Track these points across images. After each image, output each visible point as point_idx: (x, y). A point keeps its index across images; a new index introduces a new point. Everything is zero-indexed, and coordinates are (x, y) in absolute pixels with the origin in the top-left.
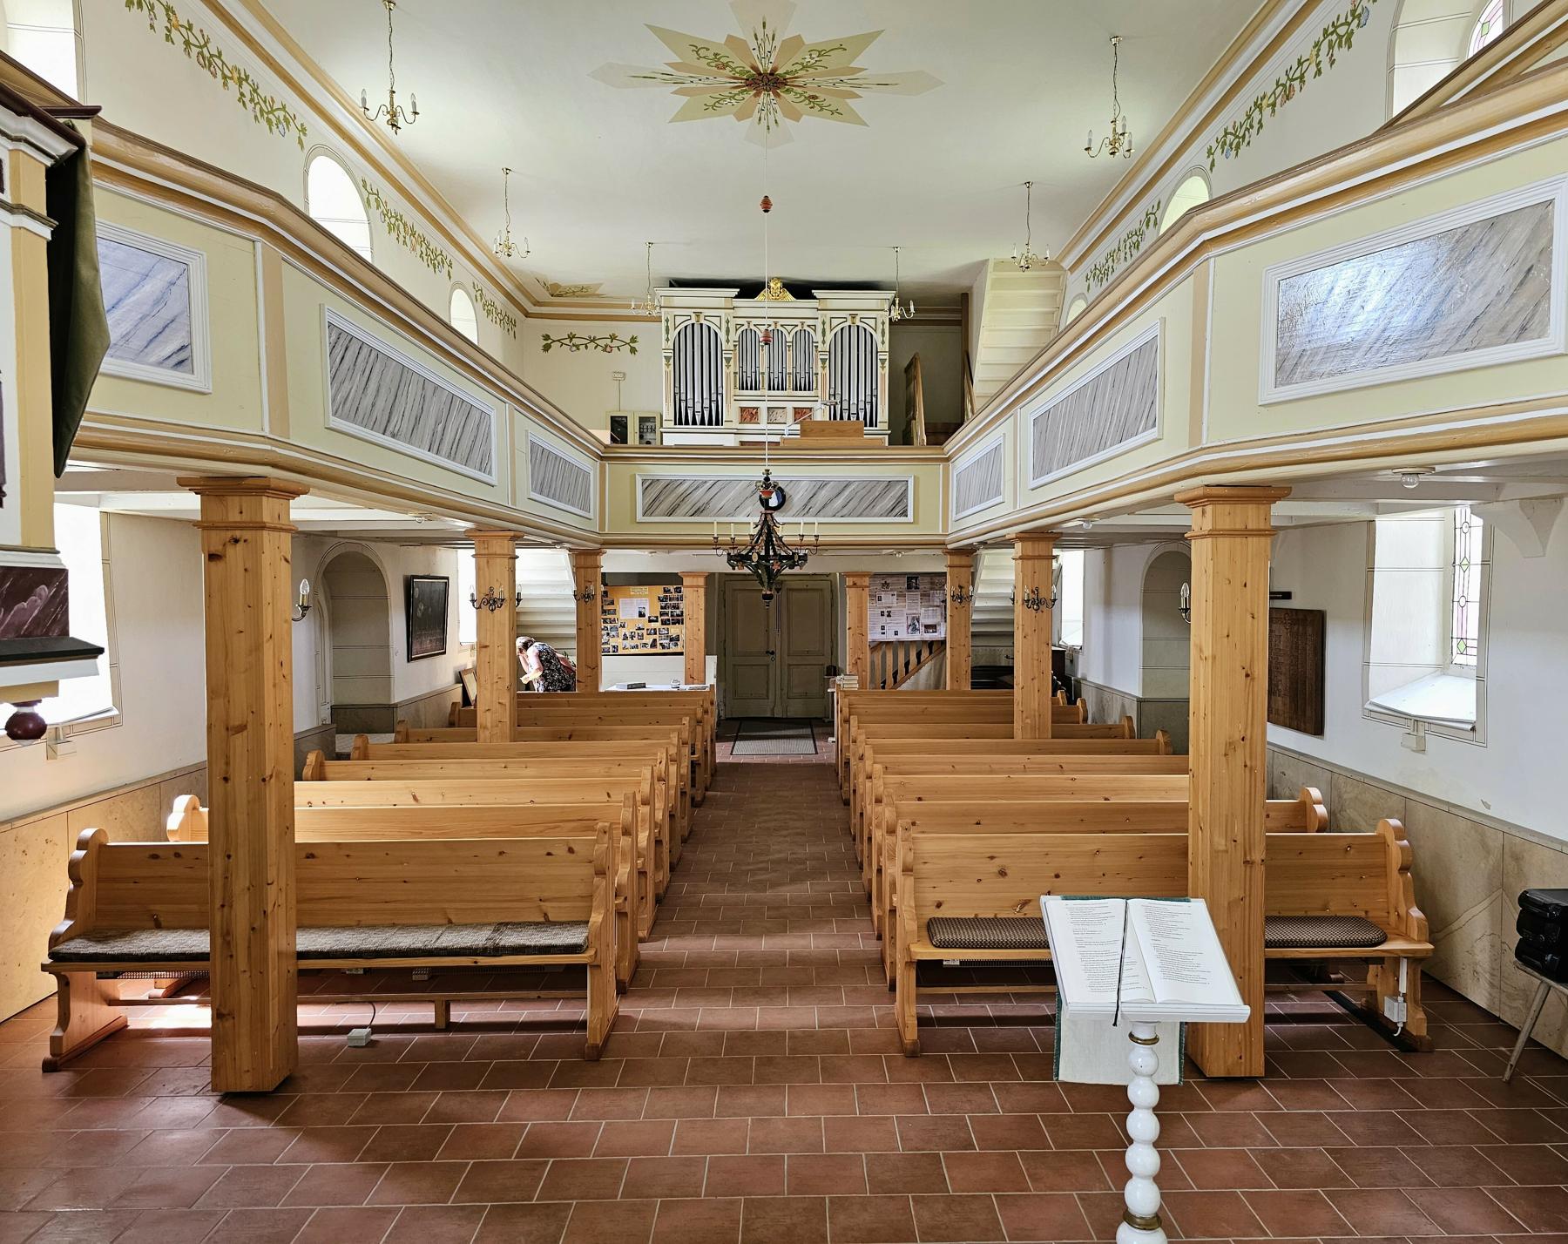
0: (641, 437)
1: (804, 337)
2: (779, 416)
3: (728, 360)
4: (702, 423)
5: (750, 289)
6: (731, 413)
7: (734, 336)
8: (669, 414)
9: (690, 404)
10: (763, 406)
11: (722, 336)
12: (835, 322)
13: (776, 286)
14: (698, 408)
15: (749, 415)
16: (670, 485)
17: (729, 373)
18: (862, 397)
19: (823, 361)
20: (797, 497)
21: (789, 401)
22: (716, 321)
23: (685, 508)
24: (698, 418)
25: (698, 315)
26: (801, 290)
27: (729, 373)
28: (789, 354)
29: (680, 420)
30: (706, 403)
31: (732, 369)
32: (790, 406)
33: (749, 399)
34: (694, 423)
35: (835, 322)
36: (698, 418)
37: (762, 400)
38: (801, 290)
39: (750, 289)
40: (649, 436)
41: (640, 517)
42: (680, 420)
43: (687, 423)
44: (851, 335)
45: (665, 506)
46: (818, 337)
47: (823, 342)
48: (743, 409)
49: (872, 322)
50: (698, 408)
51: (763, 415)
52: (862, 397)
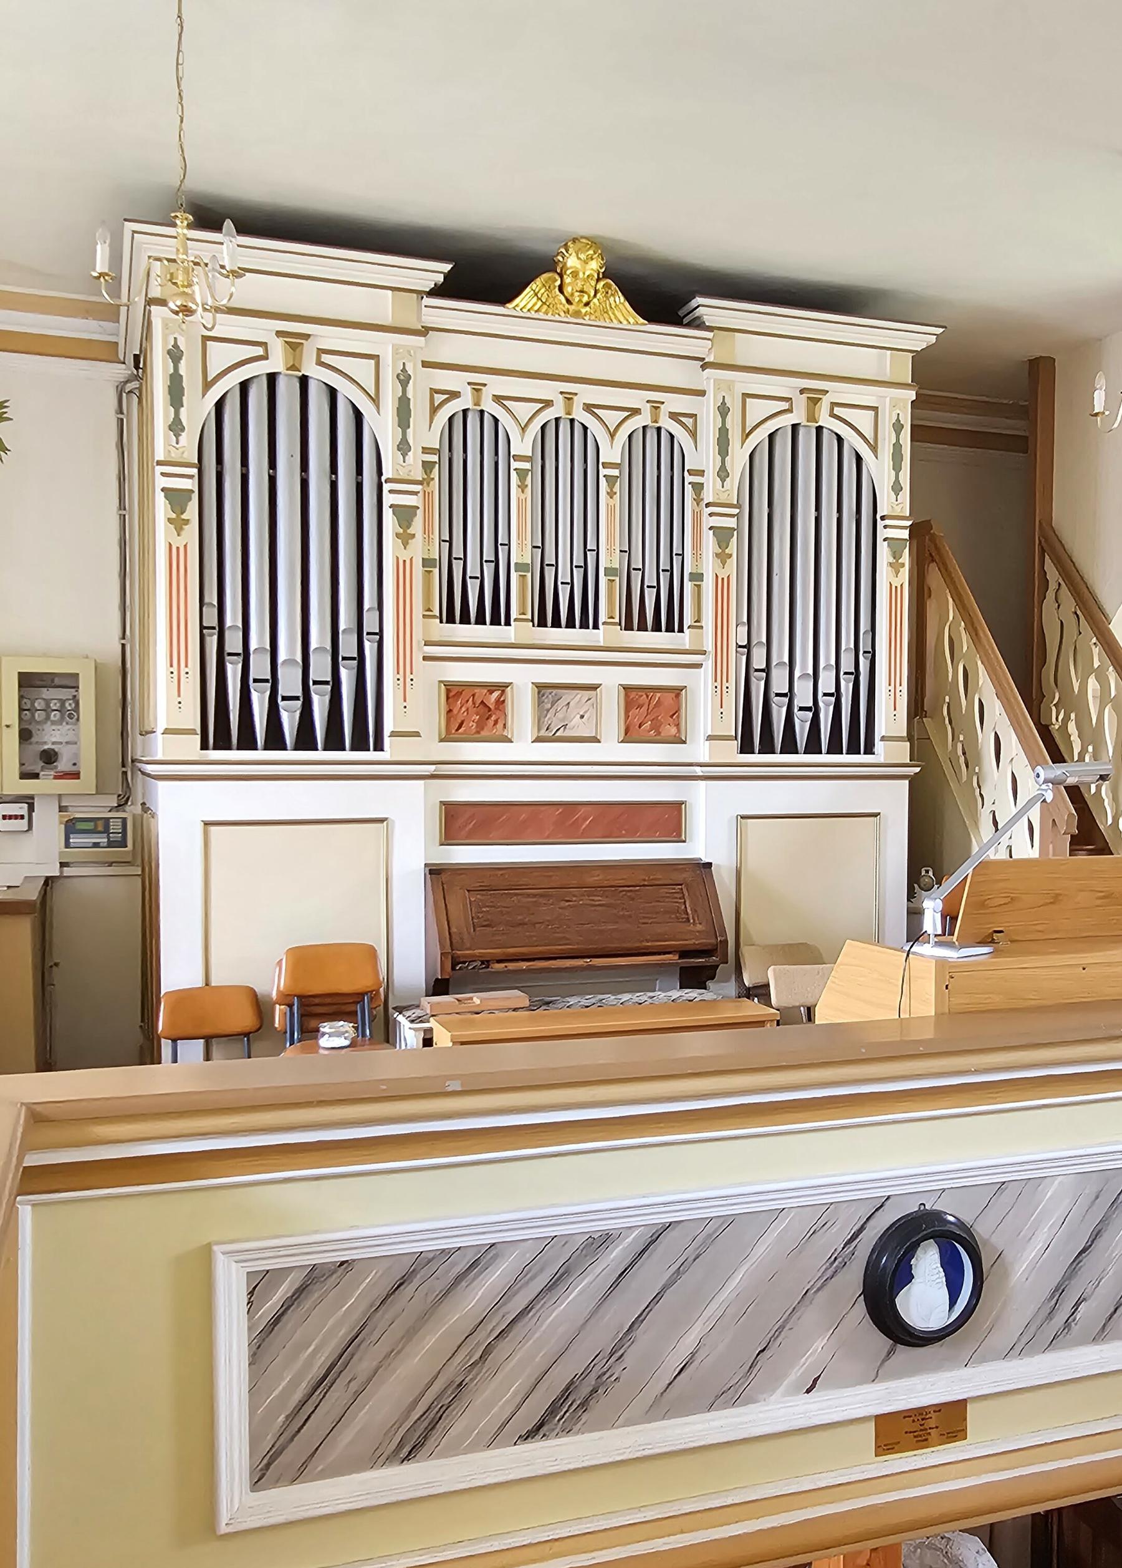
0: (25, 735)
1: (658, 452)
2: (574, 714)
3: (405, 515)
4: (306, 740)
5: (486, 273)
6: (409, 706)
7: (427, 433)
8: (171, 702)
9: (260, 667)
10: (522, 680)
11: (381, 425)
12: (758, 410)
13: (581, 266)
14: (290, 682)
15: (474, 711)
16: (418, 1280)
17: (406, 558)
18: (827, 656)
19: (722, 535)
20: (1027, 1261)
21: (609, 662)
22: (362, 371)
23: (499, 1393)
24: (289, 721)
25: (294, 343)
26: (660, 294)
27: (406, 558)
28: (611, 506)
29: (223, 728)
30: (320, 668)
31: (417, 550)
32: (612, 679)
33: (481, 655)
34: (275, 740)
35: (758, 410)
36: (289, 721)
37: (513, 659)
38: (660, 294)
39: (486, 273)
40: (52, 736)
41: (237, 1501)
42: (223, 728)
43: (247, 741)
44: (799, 458)
45: (385, 1403)
46: (702, 455)
47: (717, 473)
48: (453, 692)
49: (864, 421)
50: (290, 682)
51: (522, 710)
52: (827, 656)
